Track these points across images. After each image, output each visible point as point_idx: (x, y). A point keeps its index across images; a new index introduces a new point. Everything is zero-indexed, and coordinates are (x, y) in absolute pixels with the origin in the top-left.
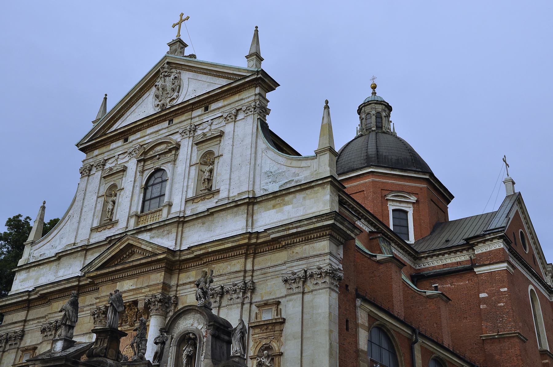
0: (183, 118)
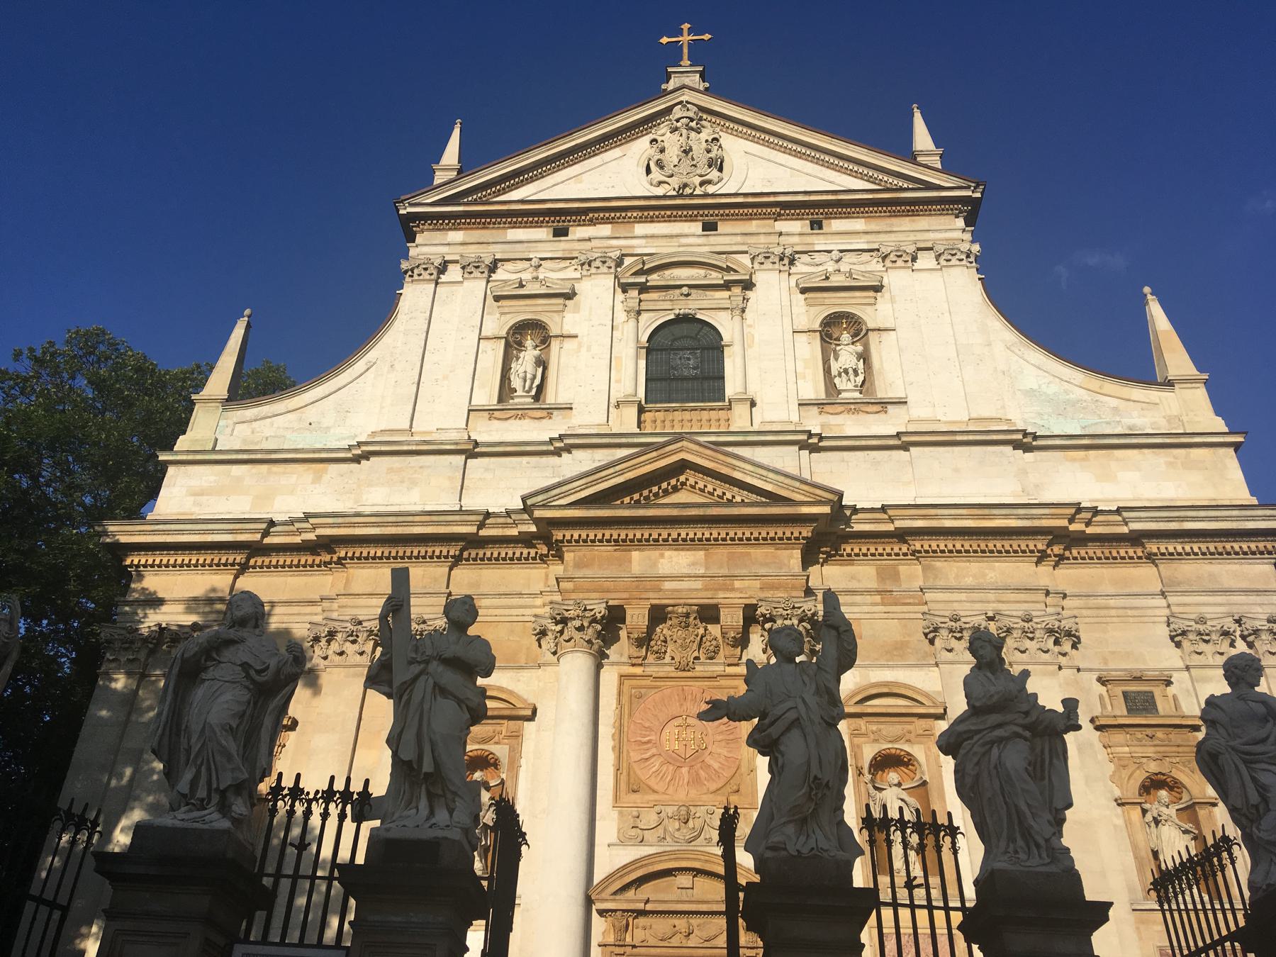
0: (754, 226)
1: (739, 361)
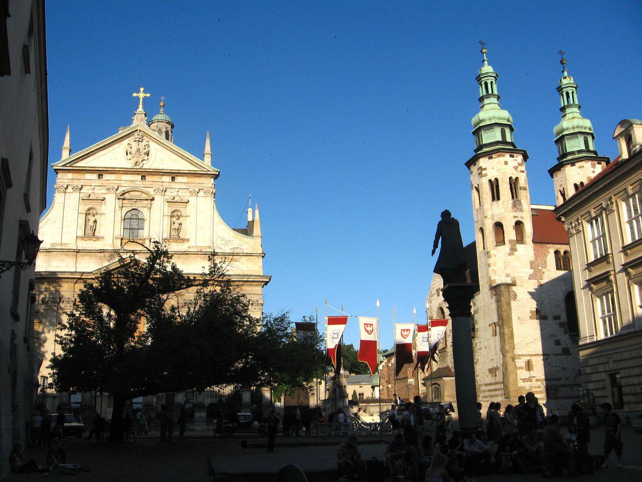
0: (156, 178)
1: (148, 224)
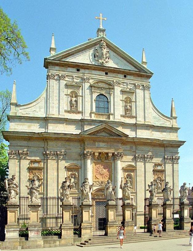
0: (114, 75)
